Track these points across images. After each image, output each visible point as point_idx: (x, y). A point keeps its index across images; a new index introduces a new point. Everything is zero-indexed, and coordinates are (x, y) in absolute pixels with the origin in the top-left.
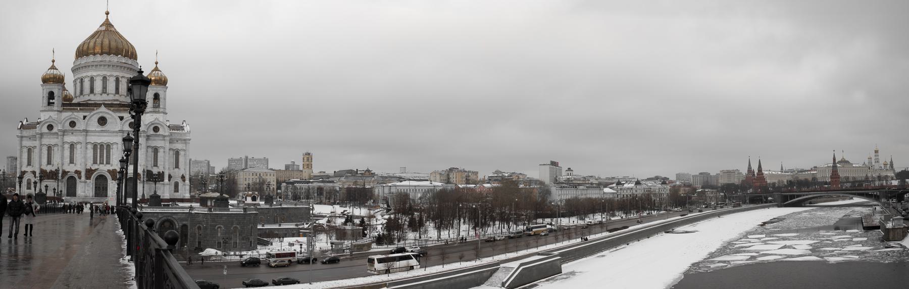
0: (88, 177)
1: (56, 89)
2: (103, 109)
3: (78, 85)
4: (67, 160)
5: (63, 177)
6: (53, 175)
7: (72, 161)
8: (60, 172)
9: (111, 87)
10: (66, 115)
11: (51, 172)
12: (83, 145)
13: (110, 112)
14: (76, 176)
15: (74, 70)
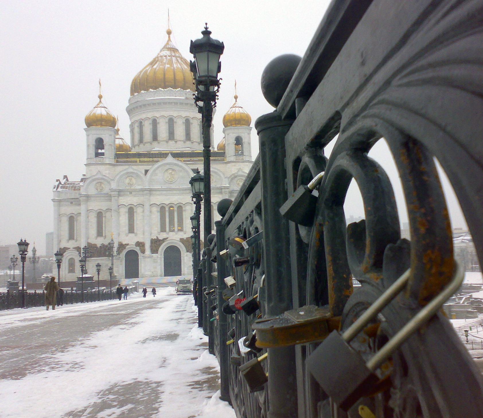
0: (154, 250)
1: (106, 134)
2: (170, 159)
3: (137, 130)
4: (126, 229)
5: (119, 252)
6: (106, 251)
7: (131, 230)
8: (116, 245)
9: (180, 131)
10: (122, 169)
11: (103, 246)
12: (147, 207)
13: (180, 163)
14: (137, 249)
15: (130, 111)
